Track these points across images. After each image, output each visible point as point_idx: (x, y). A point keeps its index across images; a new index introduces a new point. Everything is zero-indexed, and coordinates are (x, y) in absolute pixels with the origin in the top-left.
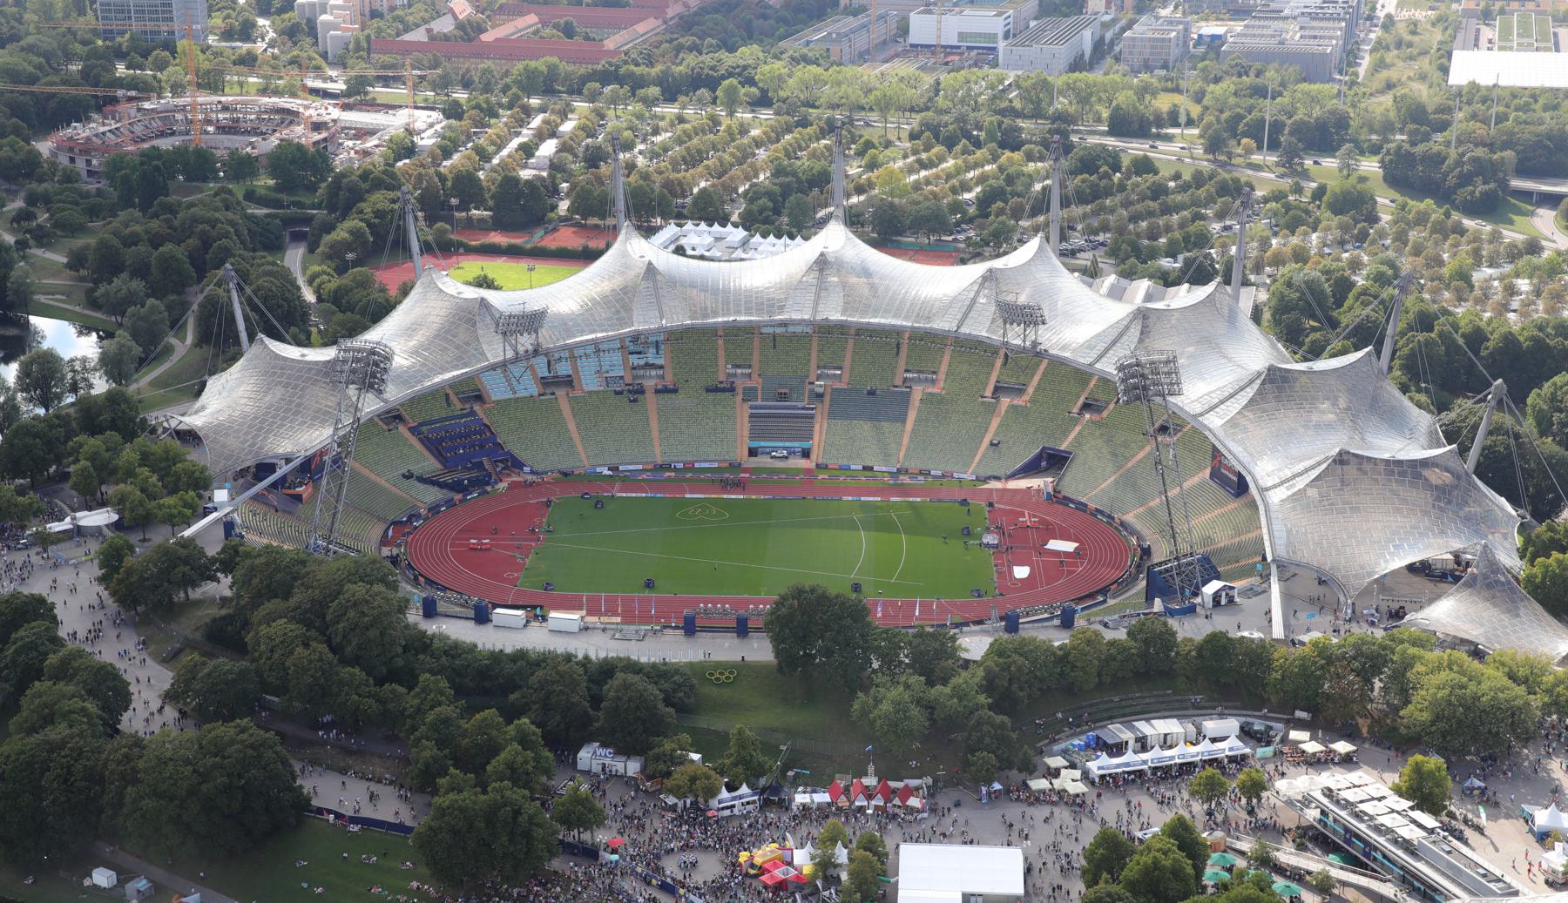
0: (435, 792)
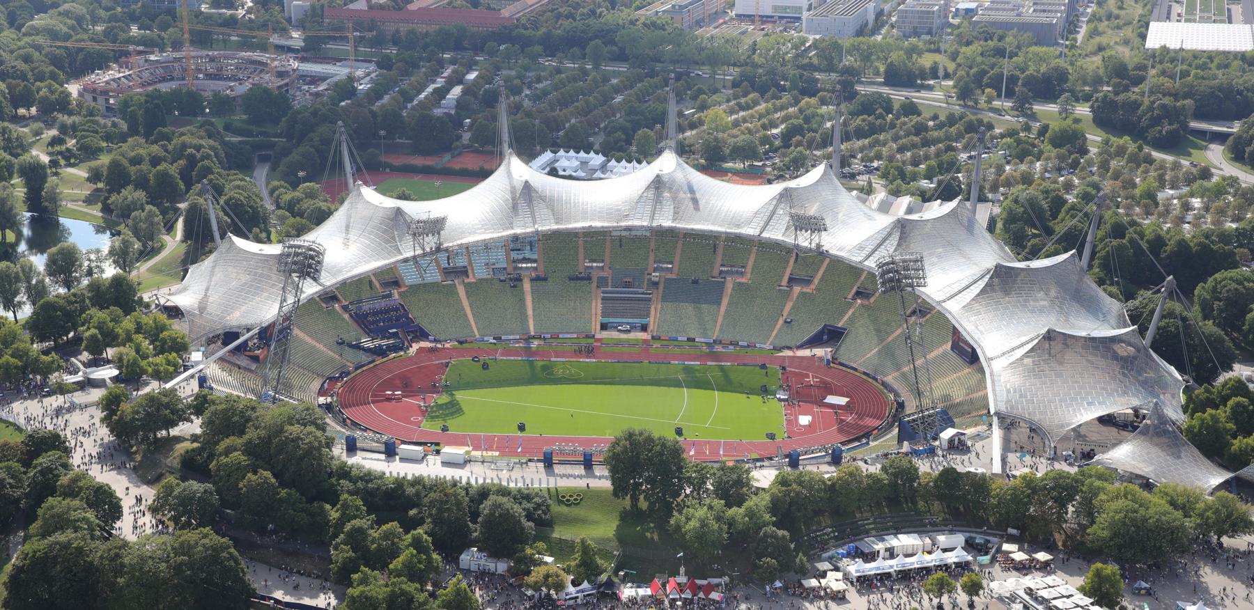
0: (350, 585)
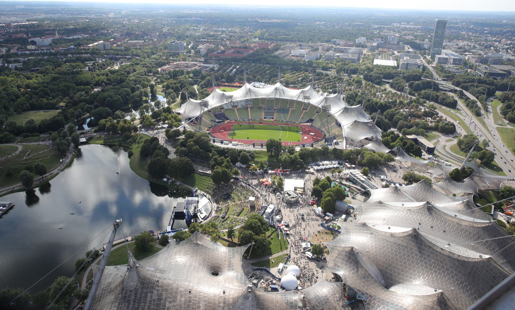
0: (214, 169)
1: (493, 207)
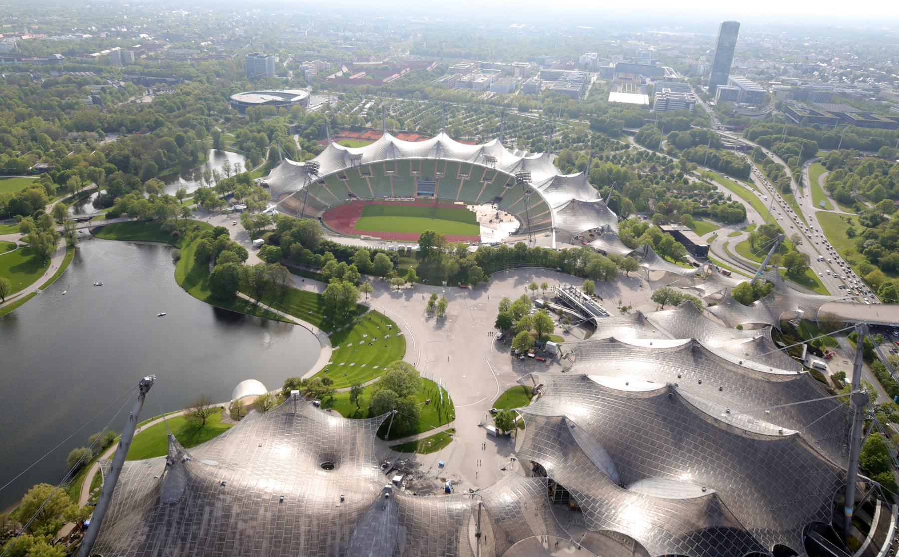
0: (328, 283)
1: (805, 347)
